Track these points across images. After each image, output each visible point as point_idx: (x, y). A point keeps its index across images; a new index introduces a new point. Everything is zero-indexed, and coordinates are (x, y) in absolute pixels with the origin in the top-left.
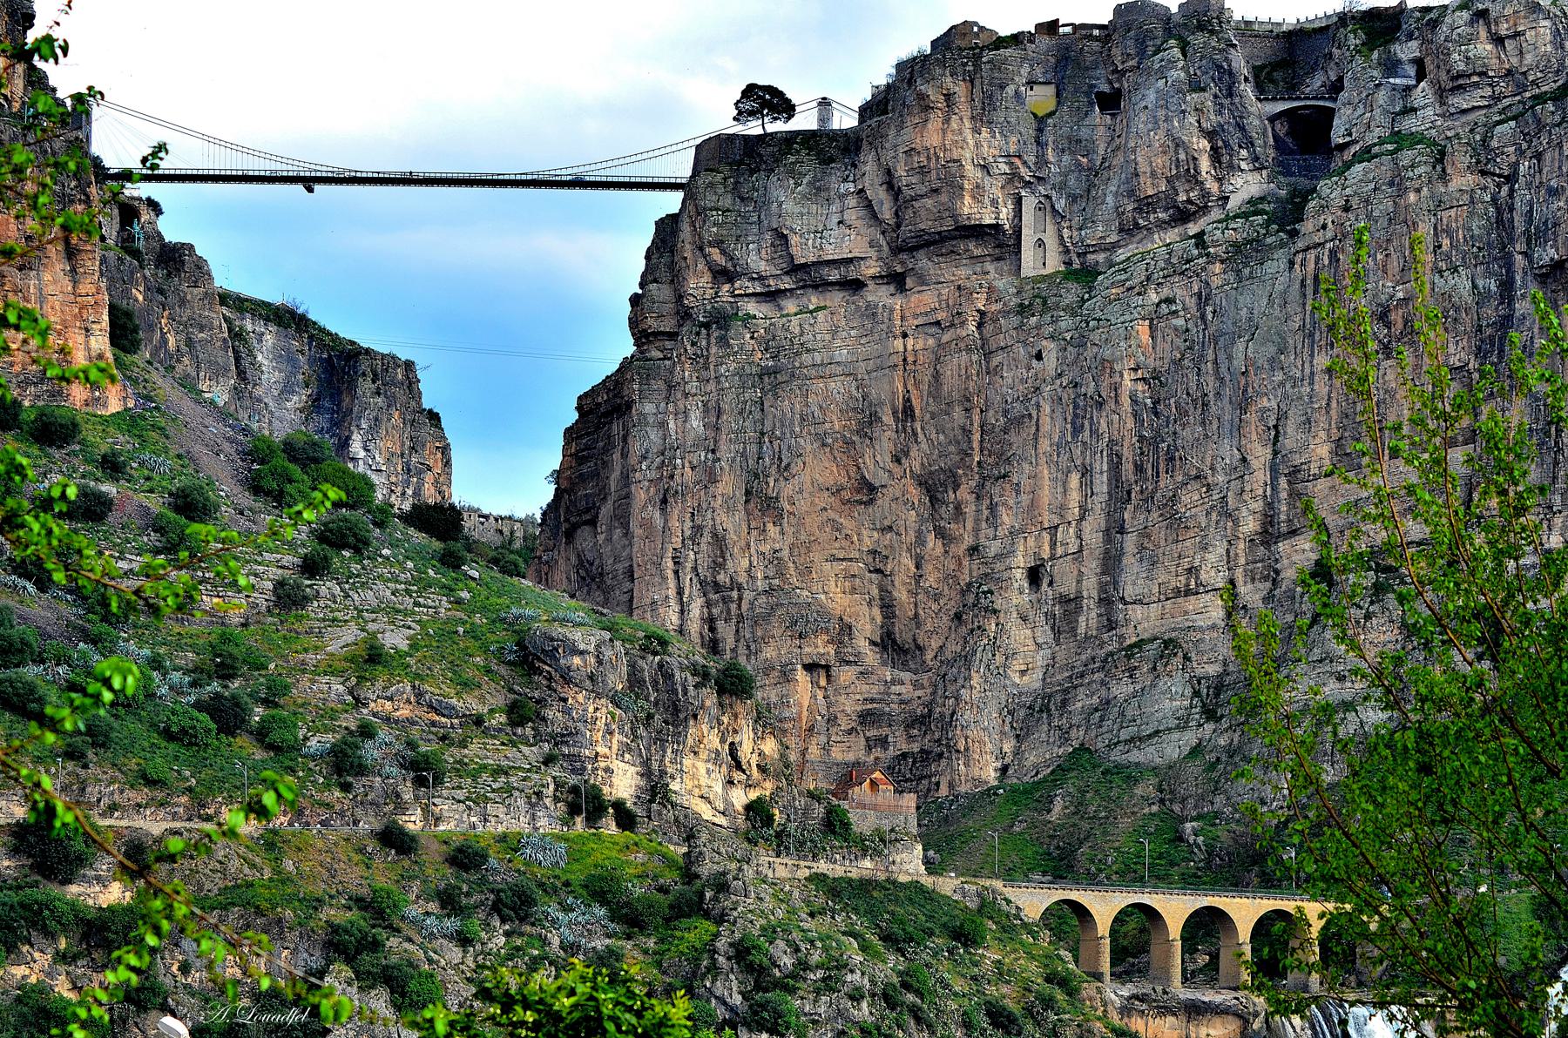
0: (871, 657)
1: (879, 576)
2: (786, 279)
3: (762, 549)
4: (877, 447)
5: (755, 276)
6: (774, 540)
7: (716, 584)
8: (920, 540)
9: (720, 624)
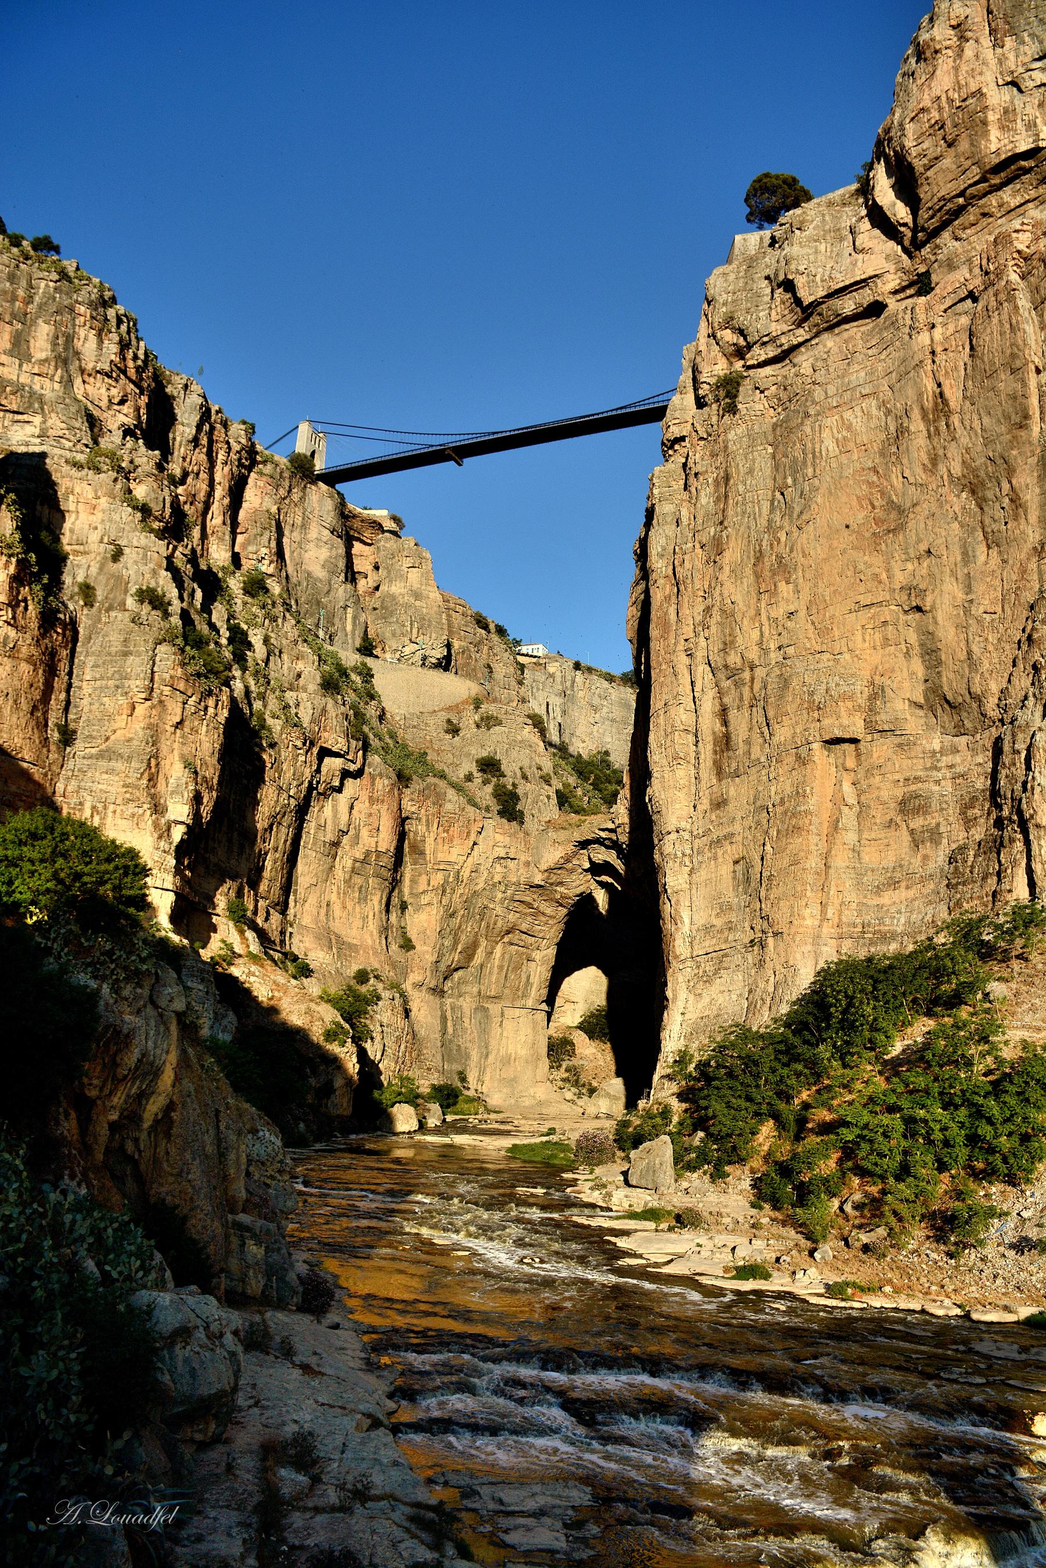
0: (914, 723)
1: (918, 615)
2: (801, 331)
3: (773, 615)
4: (905, 461)
5: (766, 339)
6: (787, 601)
7: (726, 666)
8: (967, 557)
9: (733, 714)
